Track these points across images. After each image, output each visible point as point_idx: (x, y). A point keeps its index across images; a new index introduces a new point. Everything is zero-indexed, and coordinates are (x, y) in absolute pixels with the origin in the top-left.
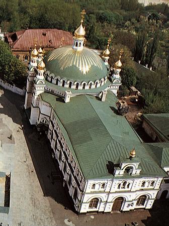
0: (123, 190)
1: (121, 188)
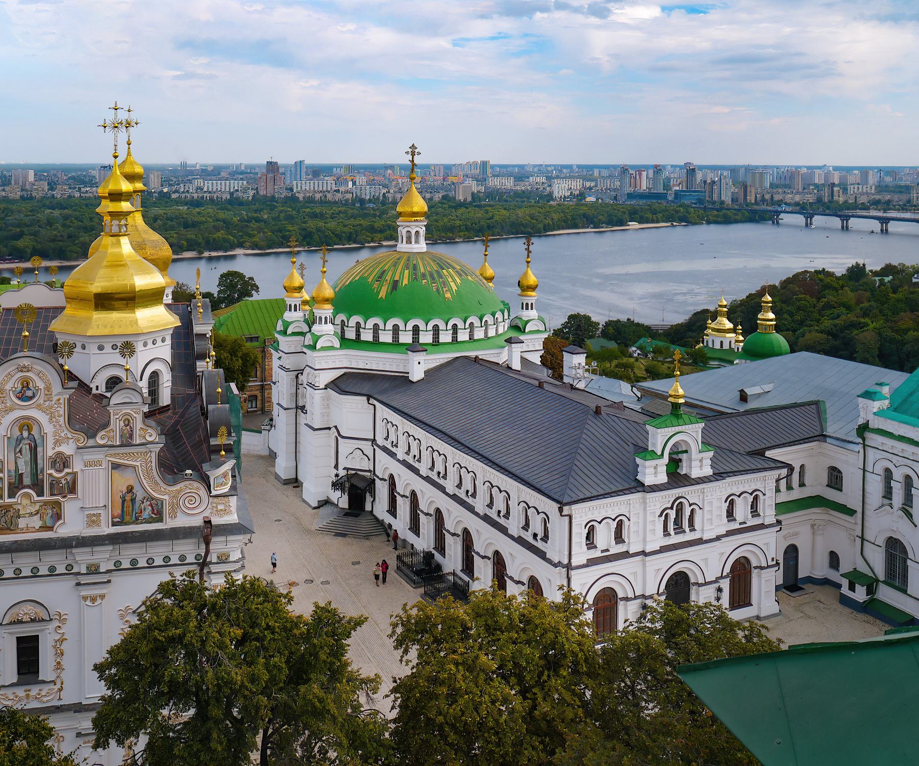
1: (672, 532)
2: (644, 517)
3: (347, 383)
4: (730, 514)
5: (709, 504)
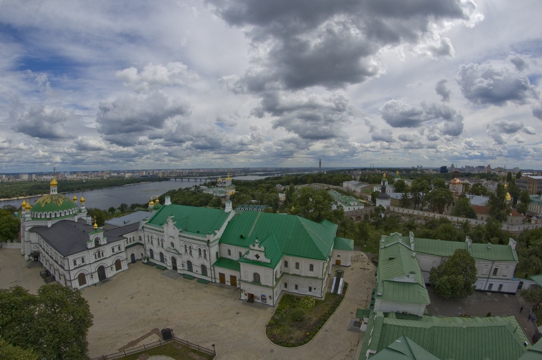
0: (100, 259)
2: (90, 256)
3: (33, 230)
4: (113, 251)
5: (107, 251)
